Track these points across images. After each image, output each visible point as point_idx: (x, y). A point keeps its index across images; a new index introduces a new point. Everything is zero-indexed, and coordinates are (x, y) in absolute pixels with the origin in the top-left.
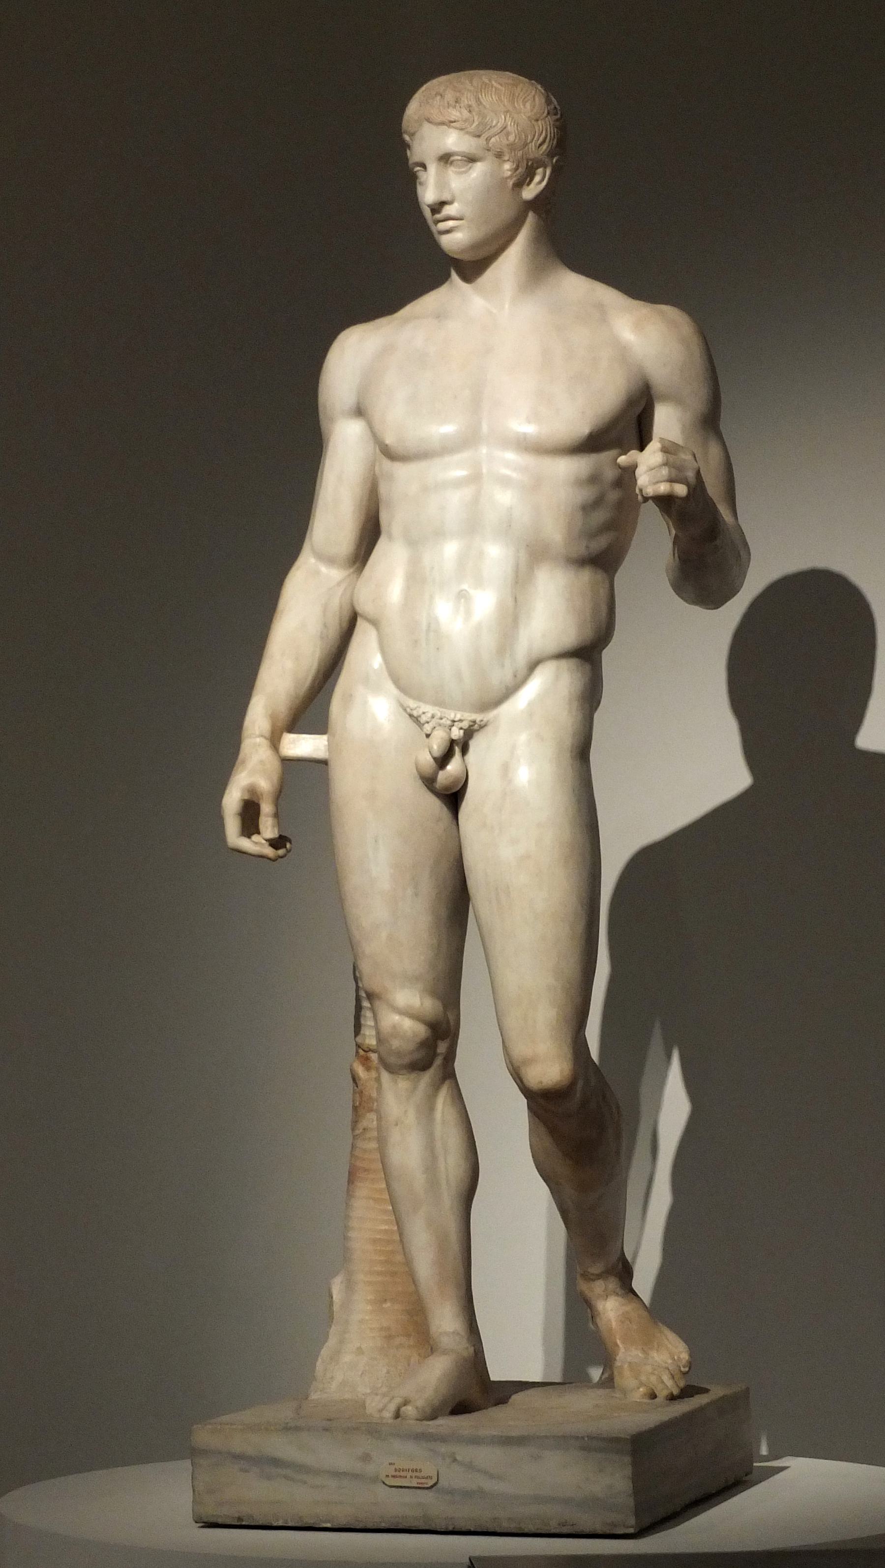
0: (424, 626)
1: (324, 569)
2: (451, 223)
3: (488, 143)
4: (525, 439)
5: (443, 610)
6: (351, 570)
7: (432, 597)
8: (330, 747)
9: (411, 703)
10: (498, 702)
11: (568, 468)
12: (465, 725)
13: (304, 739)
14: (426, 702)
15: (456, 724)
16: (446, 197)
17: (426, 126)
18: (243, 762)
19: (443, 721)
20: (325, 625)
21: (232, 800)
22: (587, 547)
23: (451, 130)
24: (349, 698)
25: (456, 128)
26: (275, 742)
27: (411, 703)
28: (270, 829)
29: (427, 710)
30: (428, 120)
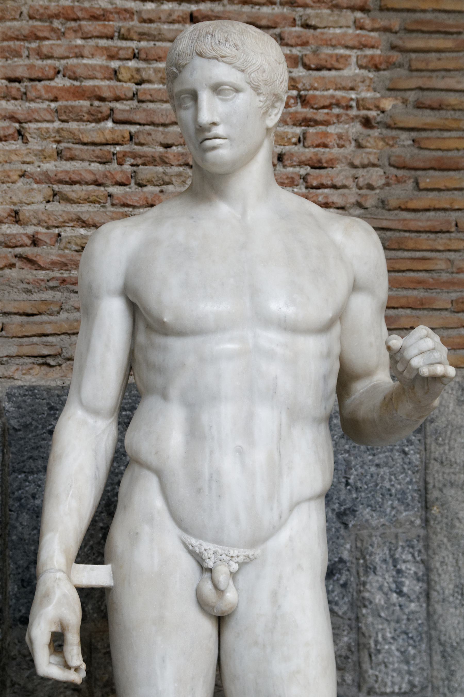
0: (207, 476)
1: (90, 420)
2: (218, 141)
3: (249, 77)
4: (285, 321)
5: (229, 466)
6: (112, 420)
7: (211, 452)
8: (115, 574)
9: (193, 541)
10: (266, 539)
11: (312, 346)
12: (241, 559)
13: (92, 570)
14: (206, 540)
15: (233, 559)
16: (216, 119)
17: (198, 61)
18: (47, 595)
19: (224, 556)
20: (97, 468)
21: (40, 634)
22: (325, 408)
23: (221, 64)
24: (135, 536)
25: (226, 62)
26: (68, 573)
27: (193, 541)
28: (75, 657)
29: (208, 548)
30: (200, 55)
